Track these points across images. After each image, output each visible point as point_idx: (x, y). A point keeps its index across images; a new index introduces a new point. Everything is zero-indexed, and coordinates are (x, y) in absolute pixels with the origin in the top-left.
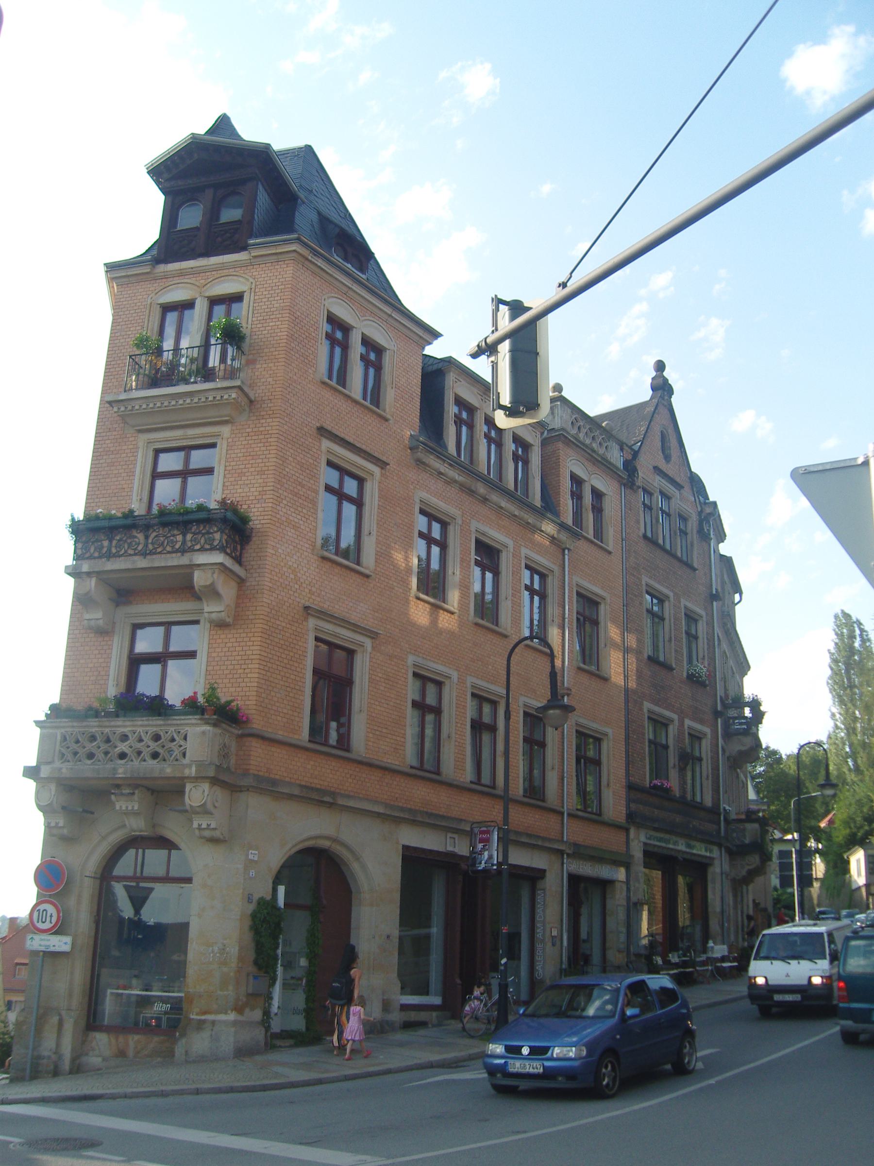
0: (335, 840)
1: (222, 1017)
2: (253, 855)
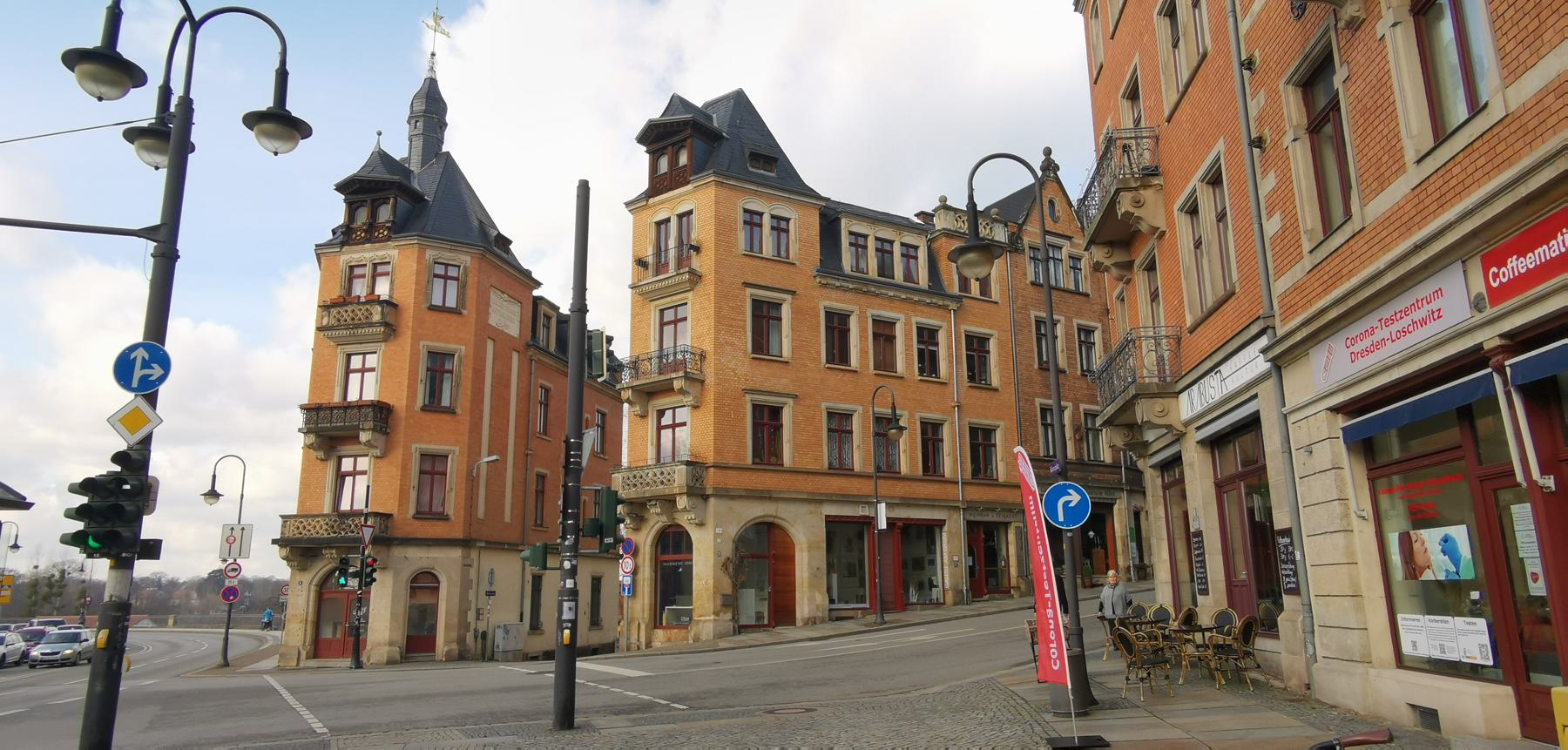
0: (775, 517)
1: (708, 618)
2: (719, 530)
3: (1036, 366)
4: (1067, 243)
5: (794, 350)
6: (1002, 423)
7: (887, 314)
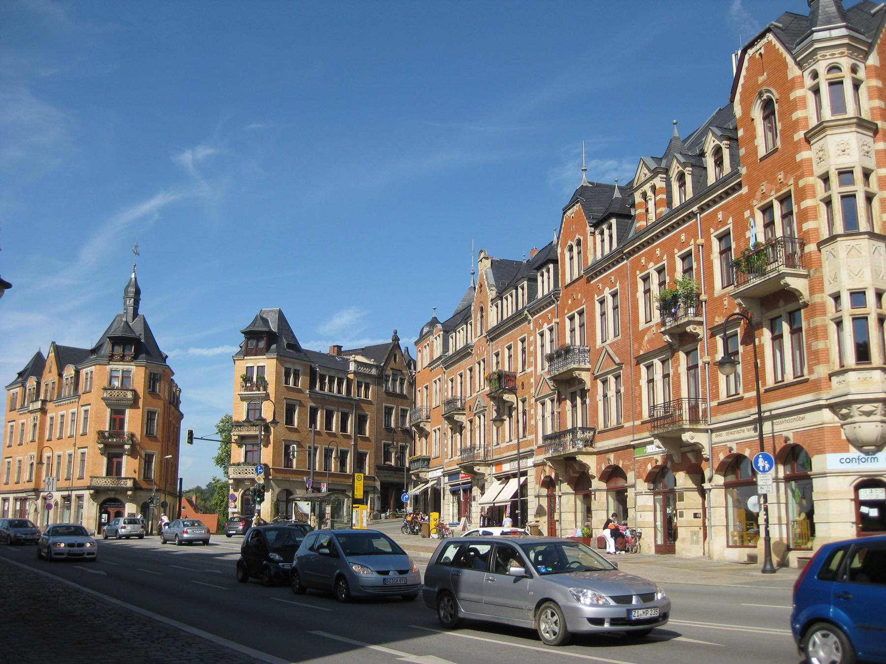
3: (383, 427)
5: (299, 423)
6: (369, 451)
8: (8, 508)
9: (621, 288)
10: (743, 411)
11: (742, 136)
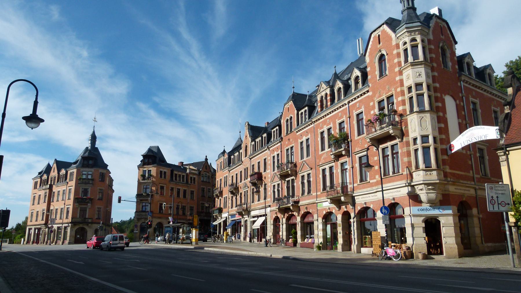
4: (208, 173)
7: (179, 188)
8: (31, 233)
9: (311, 137)
10: (370, 188)
11: (369, 71)
